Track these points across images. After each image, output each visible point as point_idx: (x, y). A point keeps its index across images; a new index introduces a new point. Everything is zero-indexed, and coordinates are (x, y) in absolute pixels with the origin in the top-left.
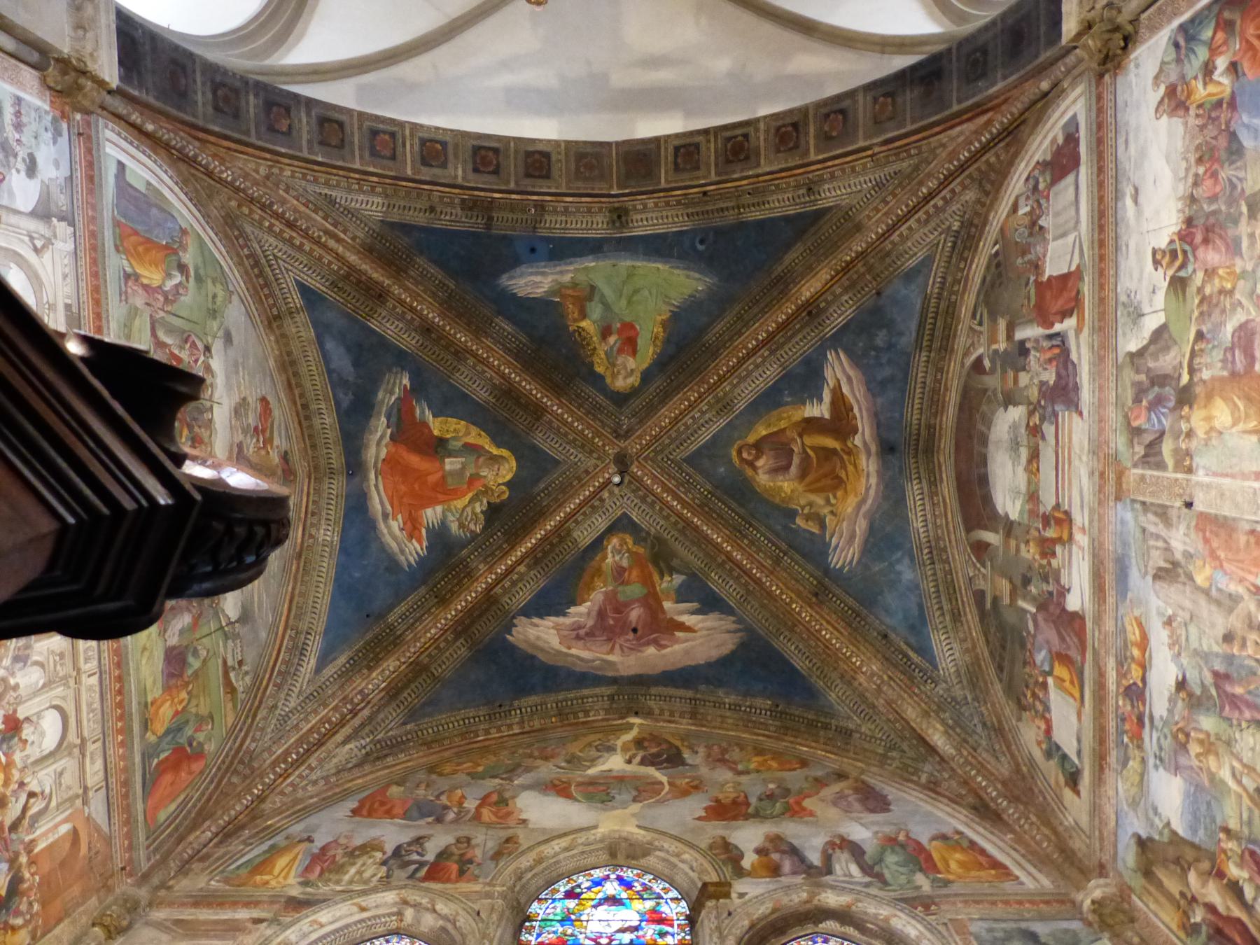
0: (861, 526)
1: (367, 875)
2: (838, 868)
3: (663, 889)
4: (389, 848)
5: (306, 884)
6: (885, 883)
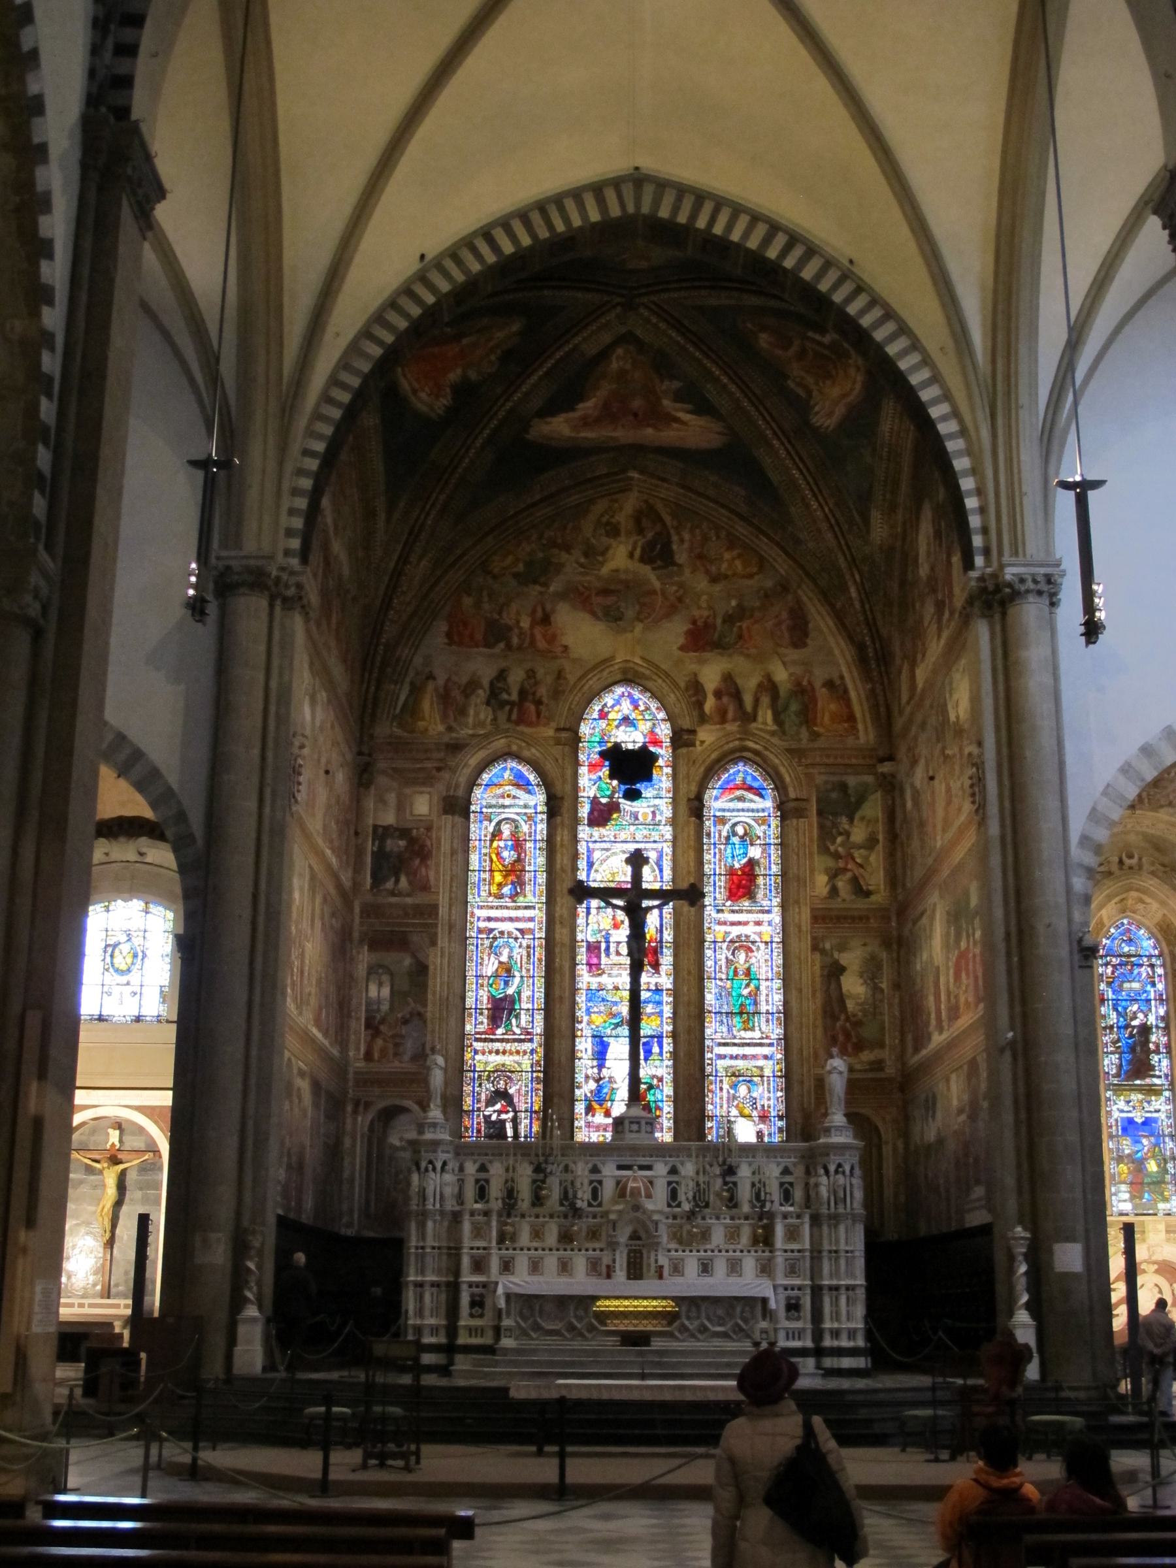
0: (840, 411)
1: (482, 716)
2: (760, 719)
4: (486, 682)
5: (450, 729)
6: (784, 733)
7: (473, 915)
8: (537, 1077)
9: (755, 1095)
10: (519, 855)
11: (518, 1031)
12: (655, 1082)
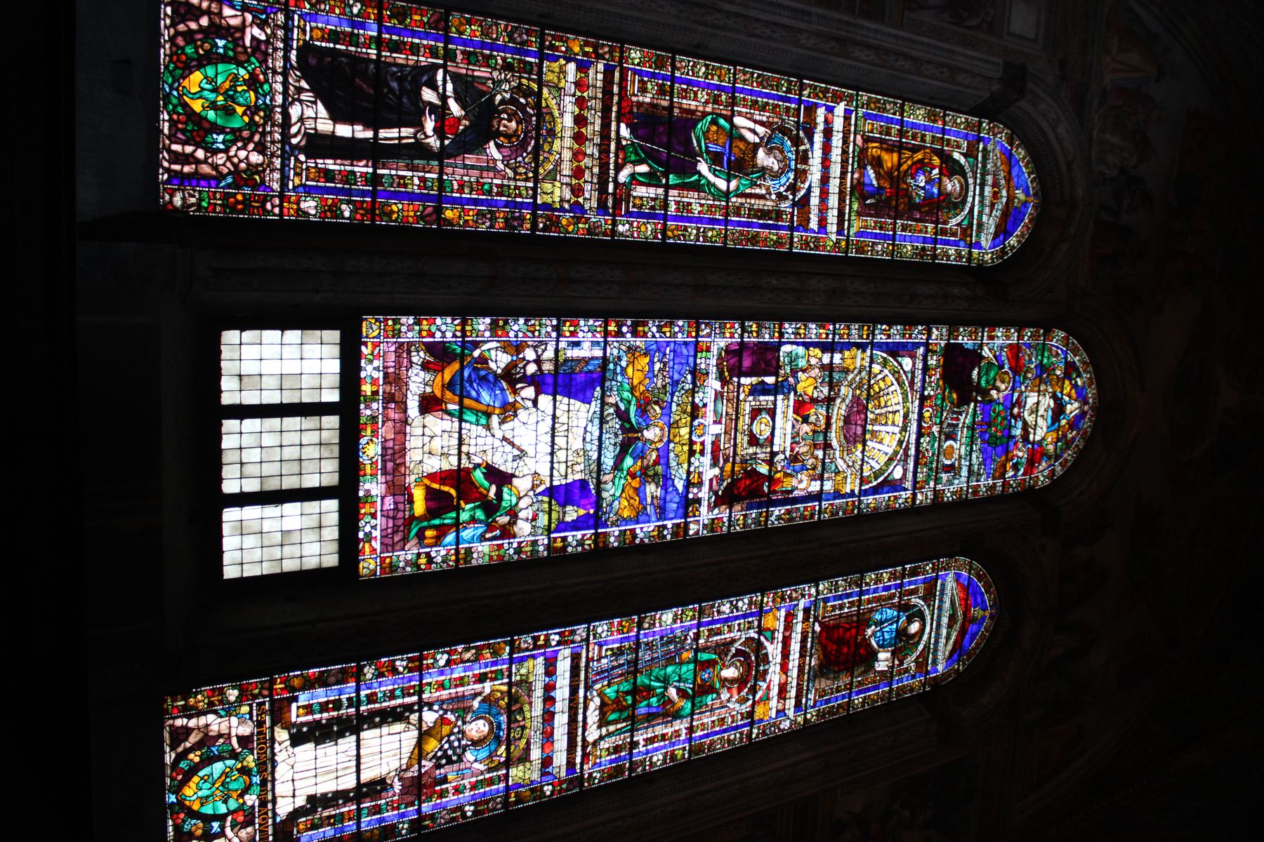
3: (1066, 460)
7: (838, 98)
8: (522, 219)
9: (469, 756)
10: (917, 207)
11: (623, 176)
12: (504, 520)
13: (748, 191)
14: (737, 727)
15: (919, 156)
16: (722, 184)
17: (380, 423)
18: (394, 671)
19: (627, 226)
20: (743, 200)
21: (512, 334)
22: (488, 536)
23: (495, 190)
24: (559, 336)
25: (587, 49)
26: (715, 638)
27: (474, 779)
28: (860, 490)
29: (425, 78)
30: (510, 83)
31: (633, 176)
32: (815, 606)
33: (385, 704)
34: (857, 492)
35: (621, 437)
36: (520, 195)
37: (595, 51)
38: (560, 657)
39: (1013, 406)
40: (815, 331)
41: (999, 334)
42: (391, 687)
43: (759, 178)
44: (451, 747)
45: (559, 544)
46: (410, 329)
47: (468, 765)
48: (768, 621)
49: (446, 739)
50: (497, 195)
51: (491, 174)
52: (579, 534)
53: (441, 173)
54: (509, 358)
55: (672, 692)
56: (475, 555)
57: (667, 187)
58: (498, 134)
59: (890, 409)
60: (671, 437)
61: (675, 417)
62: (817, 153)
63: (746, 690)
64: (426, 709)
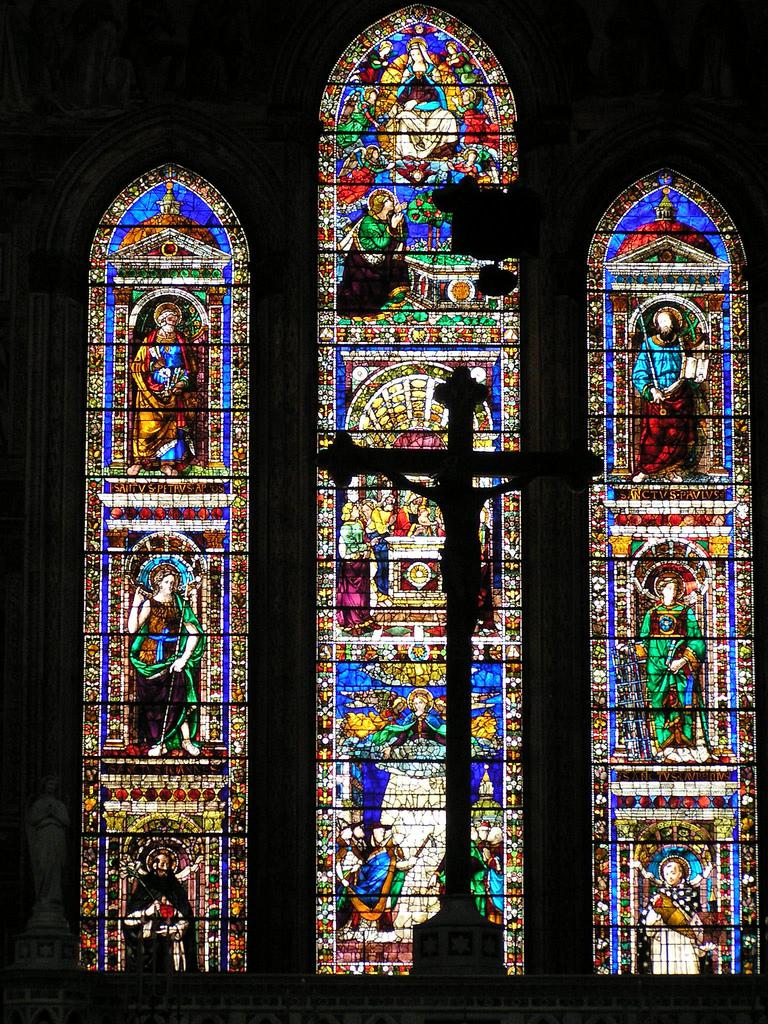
7: (96, 504)
8: (236, 847)
9: (696, 881)
10: (193, 377)
11: (194, 750)
13: (195, 611)
14: (731, 578)
15: (139, 380)
16: (192, 642)
17: (401, 964)
18: (606, 949)
19: (236, 744)
20: (204, 616)
21: (330, 852)
22: (499, 868)
23: (214, 872)
24: (331, 807)
25: (92, 792)
26: (629, 616)
27: (719, 876)
28: (492, 432)
29: (133, 935)
30: (128, 862)
31: (193, 740)
32: (613, 484)
33: (633, 958)
34: (494, 437)
35: (421, 739)
36: (217, 849)
37: (92, 784)
38: (619, 793)
39: (414, 183)
40: (326, 514)
41: (326, 221)
42: (619, 953)
43: (182, 598)
44: (683, 898)
45: (513, 799)
46: (326, 941)
47: (704, 881)
48: (621, 548)
49: (675, 903)
50: (218, 870)
51: (202, 875)
52: (506, 779)
53: (204, 919)
54: (350, 853)
55: (676, 665)
56: (514, 879)
57: (200, 704)
58: (170, 871)
59: (408, 394)
60: (424, 684)
61: (406, 682)
62: (150, 525)
63: (692, 571)
64: (644, 922)
